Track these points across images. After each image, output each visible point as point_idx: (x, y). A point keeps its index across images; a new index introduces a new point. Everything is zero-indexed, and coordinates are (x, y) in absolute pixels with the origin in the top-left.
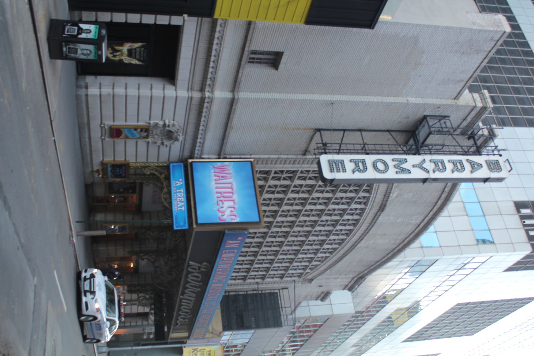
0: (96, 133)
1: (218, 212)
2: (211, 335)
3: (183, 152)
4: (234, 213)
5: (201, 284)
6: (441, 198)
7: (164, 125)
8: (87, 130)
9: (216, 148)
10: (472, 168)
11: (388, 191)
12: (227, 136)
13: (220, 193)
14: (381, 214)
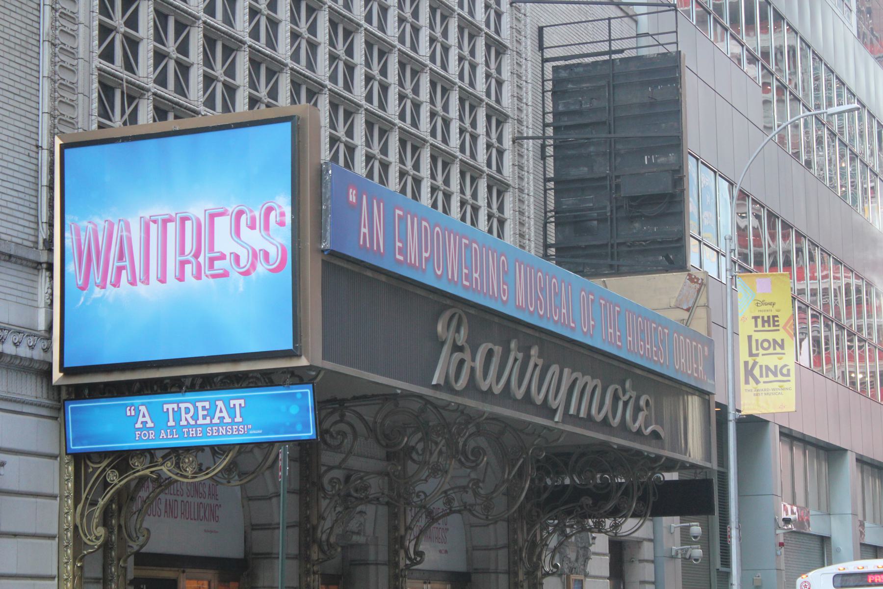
1: (253, 275)
2: (700, 313)
3: (23, 402)
4: (258, 214)
5: (513, 345)
13: (183, 264)
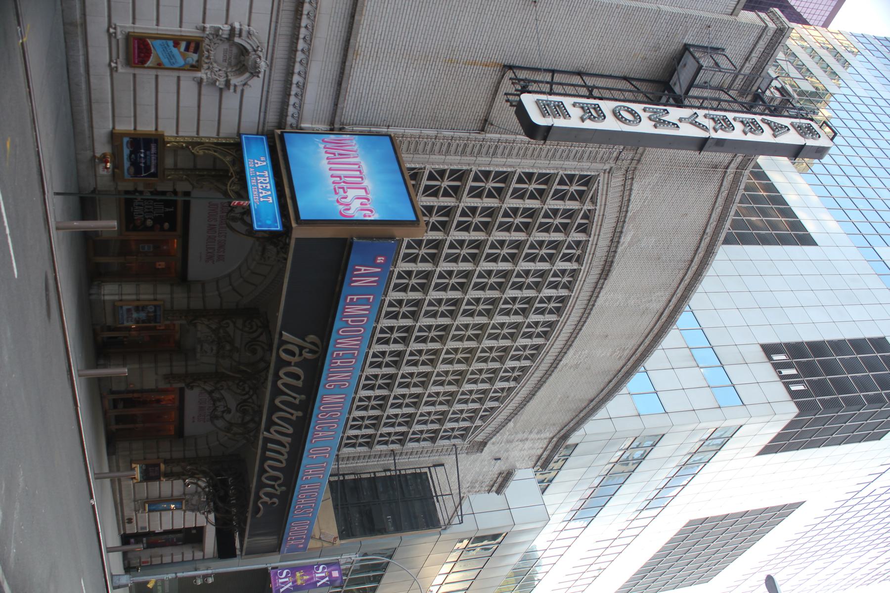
0: (100, 52)
2: (319, 544)
3: (265, 112)
4: (368, 207)
6: (700, 250)
7: (233, 29)
8: (80, 44)
9: (326, 104)
10: (773, 130)
11: (618, 230)
12: (347, 71)
13: (340, 177)
14: (603, 284)
